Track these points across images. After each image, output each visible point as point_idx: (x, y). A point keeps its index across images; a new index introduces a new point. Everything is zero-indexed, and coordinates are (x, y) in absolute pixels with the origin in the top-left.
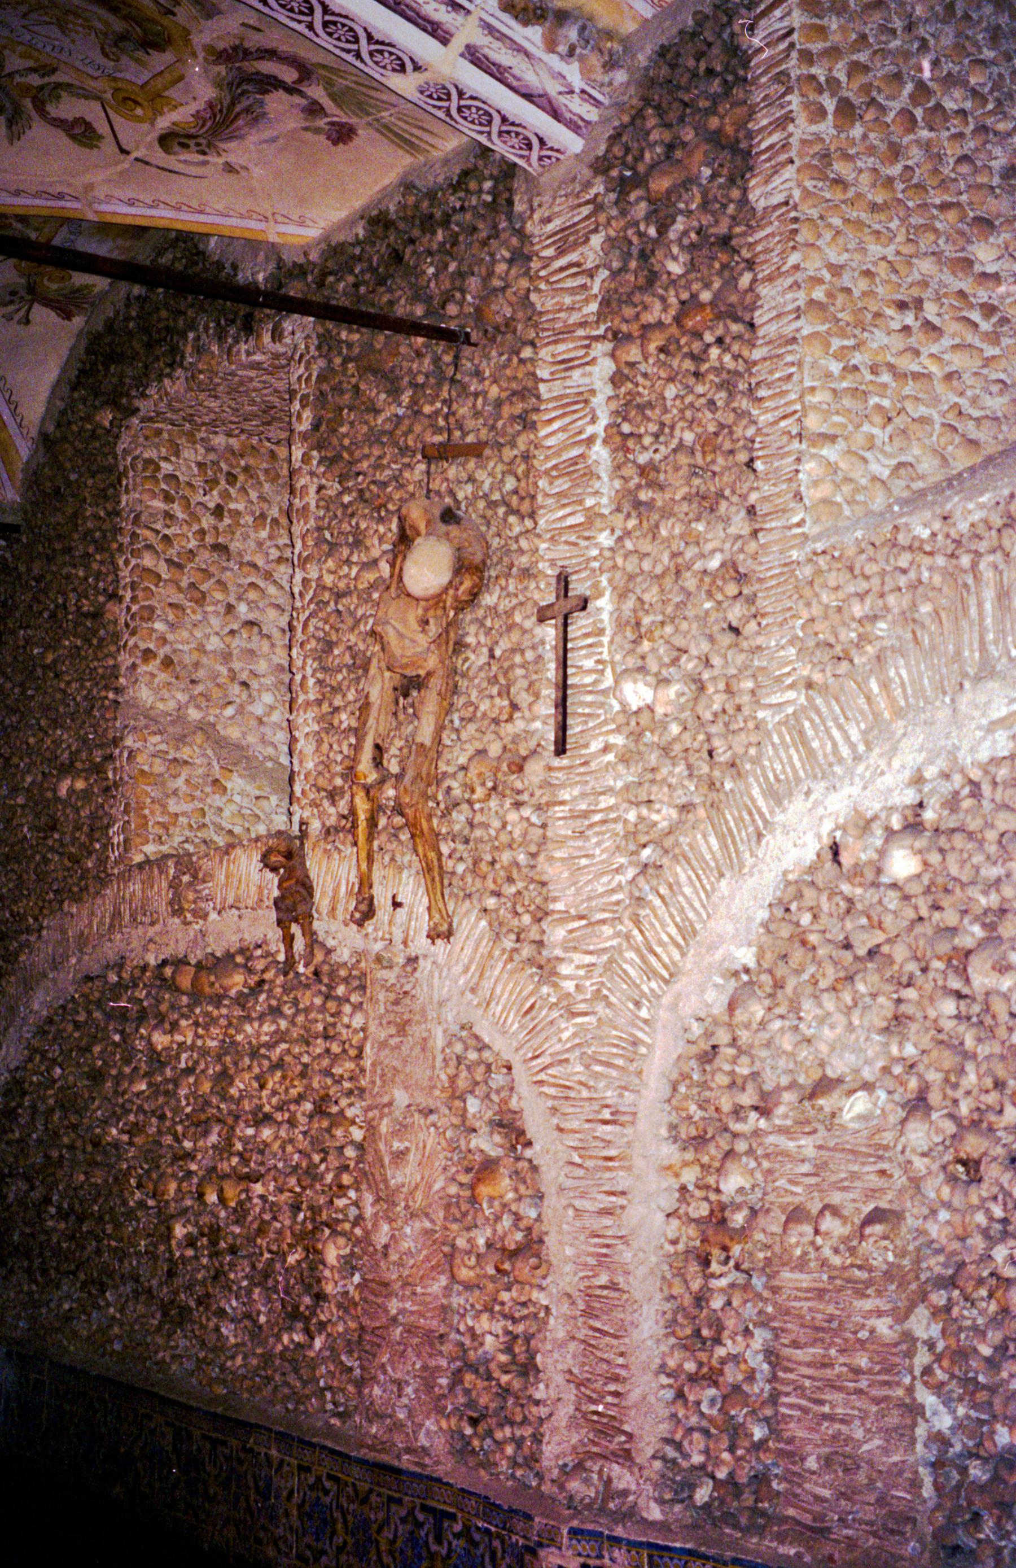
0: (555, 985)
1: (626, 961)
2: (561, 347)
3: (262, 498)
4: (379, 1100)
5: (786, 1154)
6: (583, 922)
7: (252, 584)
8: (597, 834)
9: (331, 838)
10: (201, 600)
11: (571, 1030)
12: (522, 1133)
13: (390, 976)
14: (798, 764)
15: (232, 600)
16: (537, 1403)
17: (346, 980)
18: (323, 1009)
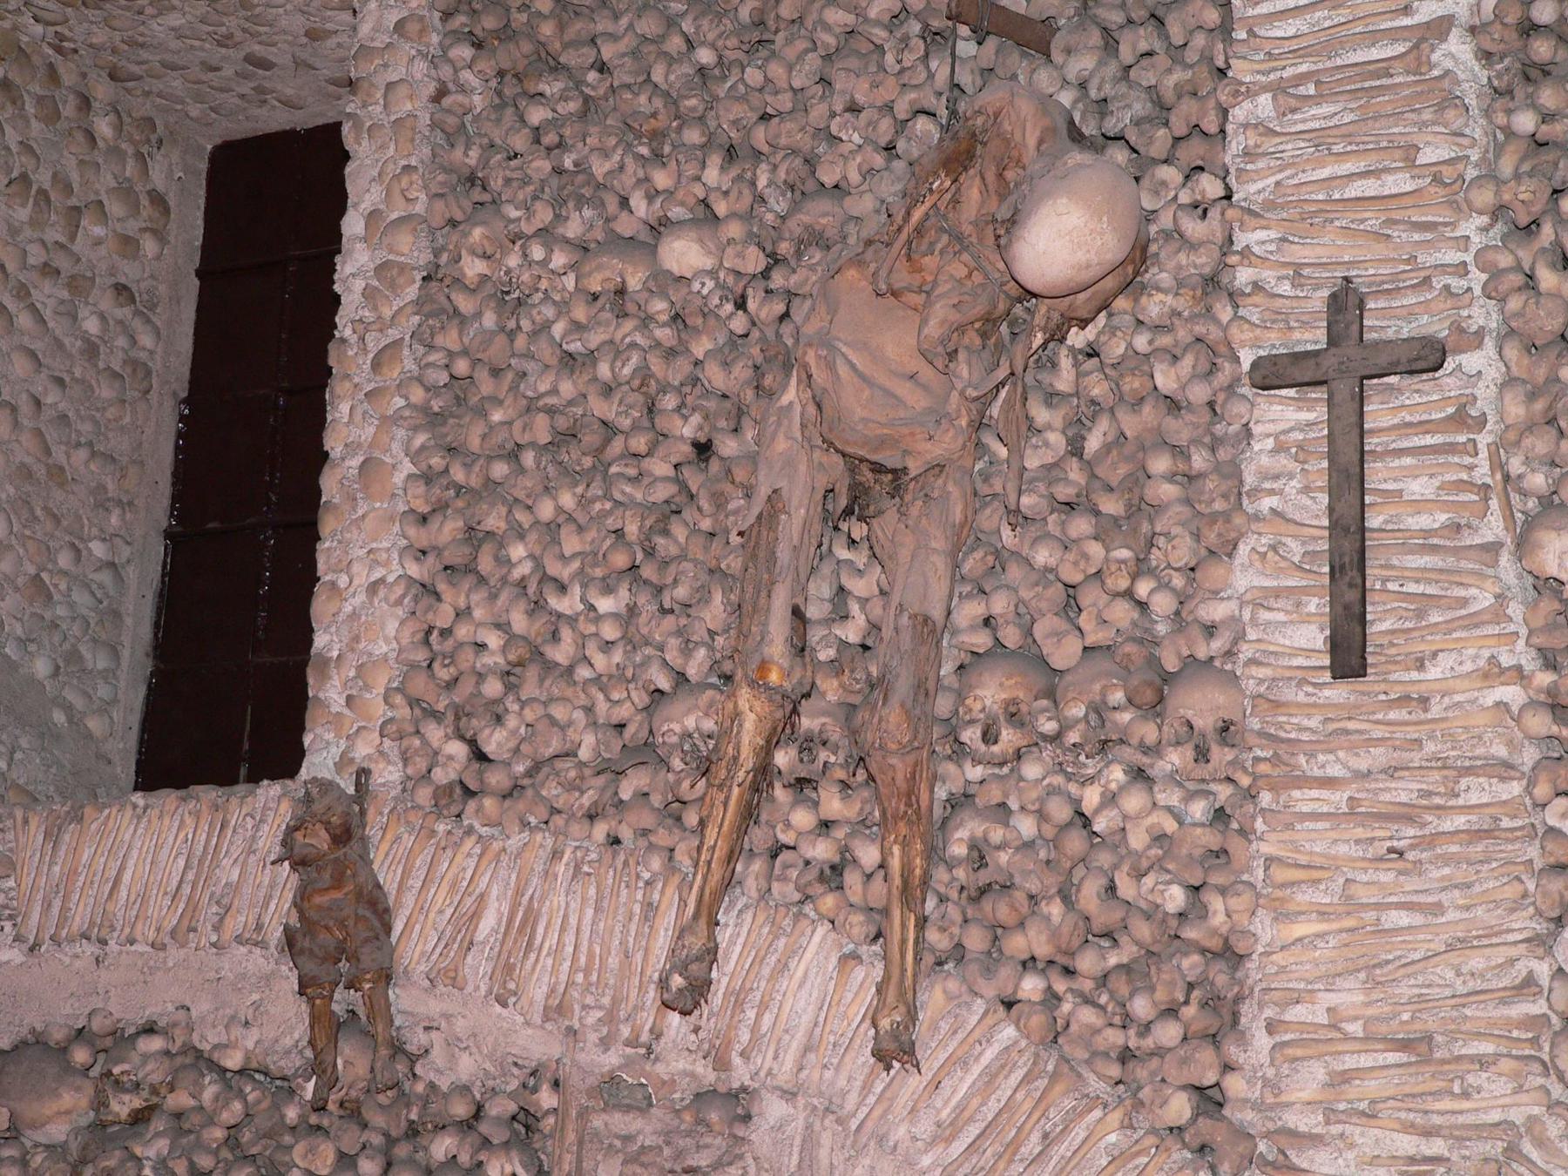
3: (26, 147)
6: (1393, 1057)
8: (1447, 860)
13: (644, 1129)
17: (468, 1125)
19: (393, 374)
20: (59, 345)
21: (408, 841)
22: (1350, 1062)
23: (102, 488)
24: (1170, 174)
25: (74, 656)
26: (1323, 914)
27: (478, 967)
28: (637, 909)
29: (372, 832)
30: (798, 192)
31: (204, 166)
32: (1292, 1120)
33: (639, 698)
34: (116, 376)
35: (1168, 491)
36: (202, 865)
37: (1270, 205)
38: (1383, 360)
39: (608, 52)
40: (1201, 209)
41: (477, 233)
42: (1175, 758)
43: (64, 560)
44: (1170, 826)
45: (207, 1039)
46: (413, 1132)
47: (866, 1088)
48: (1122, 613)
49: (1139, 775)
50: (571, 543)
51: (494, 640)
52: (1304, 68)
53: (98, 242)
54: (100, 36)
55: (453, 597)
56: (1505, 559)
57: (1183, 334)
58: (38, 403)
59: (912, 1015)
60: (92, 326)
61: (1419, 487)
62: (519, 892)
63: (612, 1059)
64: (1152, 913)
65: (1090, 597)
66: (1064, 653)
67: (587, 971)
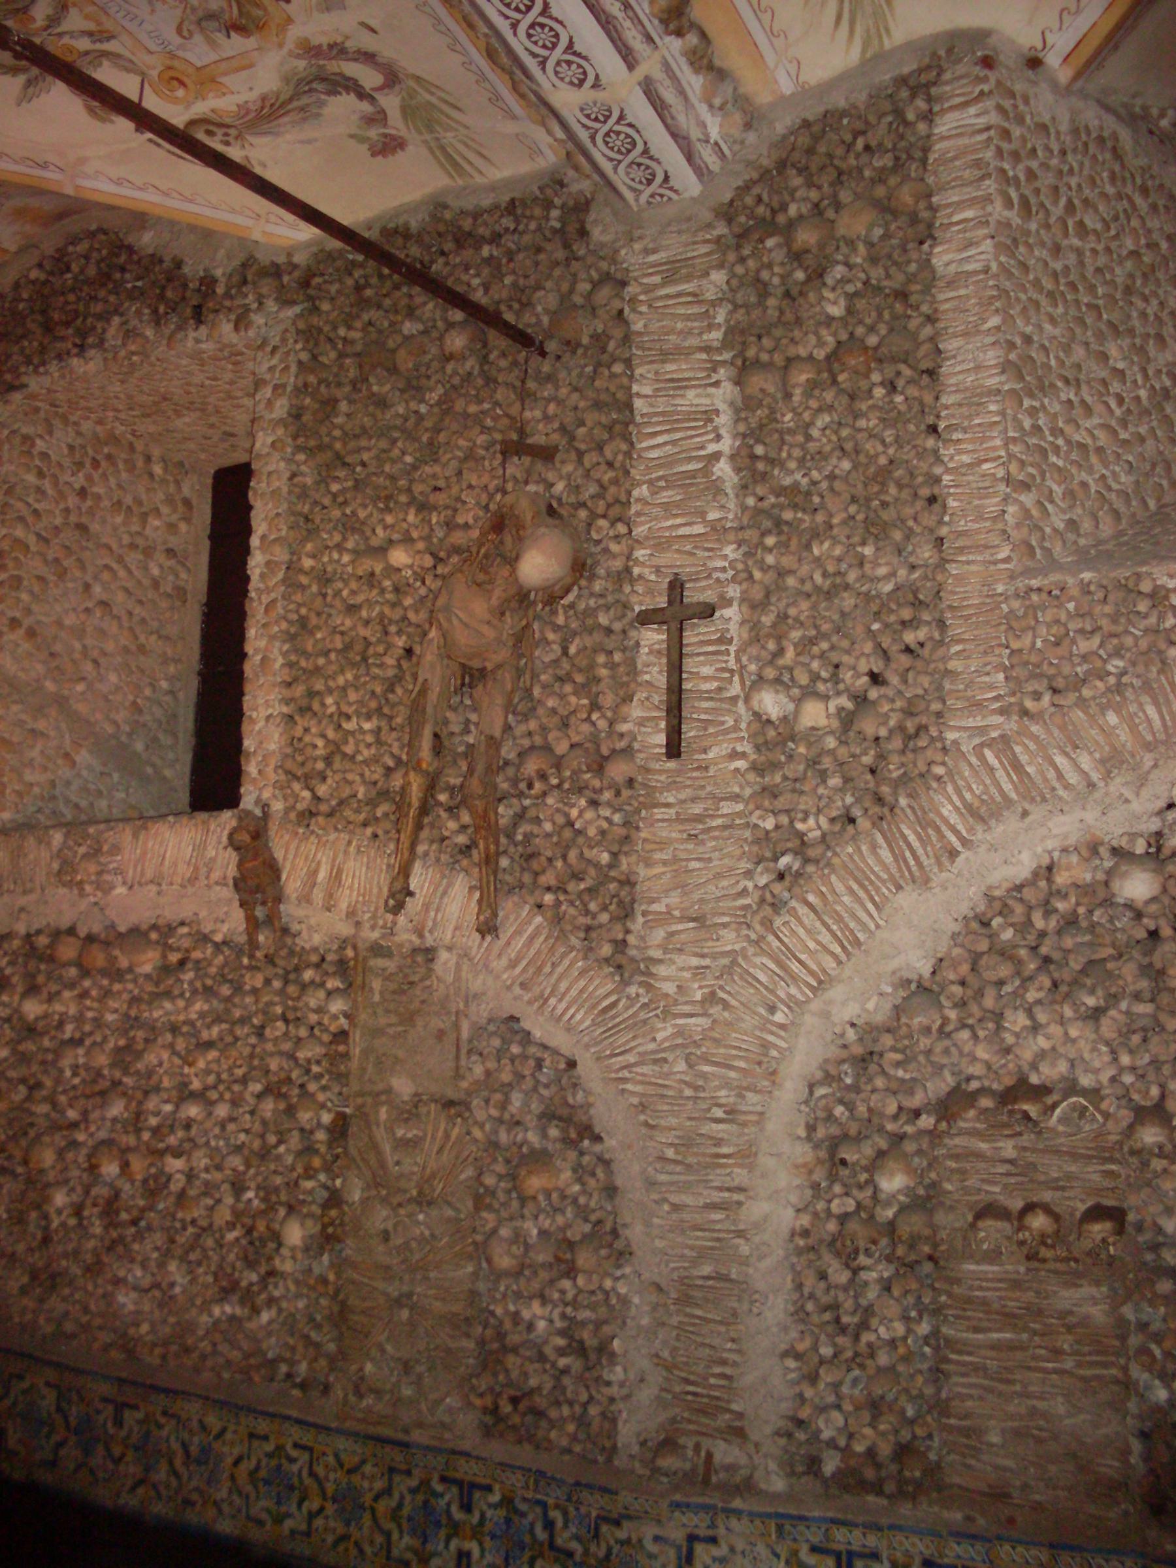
0: (649, 987)
1: (755, 966)
2: (670, 367)
3: (120, 486)
5: (979, 1155)
7: (106, 566)
8: (715, 838)
10: (62, 574)
11: (670, 1031)
13: (390, 965)
14: (1007, 787)
15: (88, 579)
16: (608, 1384)
17: (318, 966)
18: (282, 992)
19: (273, 615)
20: (139, 582)
22: (674, 928)
24: (602, 522)
25: (155, 739)
26: (665, 863)
27: (318, 896)
29: (272, 833)
30: (450, 525)
31: (210, 481)
33: (380, 770)
35: (604, 672)
36: (200, 848)
37: (647, 538)
38: (690, 612)
39: (365, 456)
40: (617, 537)
41: (309, 546)
42: (607, 795)
43: (148, 692)
44: (605, 825)
45: (207, 928)
46: (297, 969)
48: (586, 728)
49: (594, 803)
50: (353, 696)
51: (320, 743)
56: (741, 704)
57: (610, 599)
58: (130, 614)
59: (495, 915)
60: (156, 571)
61: (706, 671)
63: (375, 935)
64: (597, 866)
65: (573, 720)
66: (562, 748)
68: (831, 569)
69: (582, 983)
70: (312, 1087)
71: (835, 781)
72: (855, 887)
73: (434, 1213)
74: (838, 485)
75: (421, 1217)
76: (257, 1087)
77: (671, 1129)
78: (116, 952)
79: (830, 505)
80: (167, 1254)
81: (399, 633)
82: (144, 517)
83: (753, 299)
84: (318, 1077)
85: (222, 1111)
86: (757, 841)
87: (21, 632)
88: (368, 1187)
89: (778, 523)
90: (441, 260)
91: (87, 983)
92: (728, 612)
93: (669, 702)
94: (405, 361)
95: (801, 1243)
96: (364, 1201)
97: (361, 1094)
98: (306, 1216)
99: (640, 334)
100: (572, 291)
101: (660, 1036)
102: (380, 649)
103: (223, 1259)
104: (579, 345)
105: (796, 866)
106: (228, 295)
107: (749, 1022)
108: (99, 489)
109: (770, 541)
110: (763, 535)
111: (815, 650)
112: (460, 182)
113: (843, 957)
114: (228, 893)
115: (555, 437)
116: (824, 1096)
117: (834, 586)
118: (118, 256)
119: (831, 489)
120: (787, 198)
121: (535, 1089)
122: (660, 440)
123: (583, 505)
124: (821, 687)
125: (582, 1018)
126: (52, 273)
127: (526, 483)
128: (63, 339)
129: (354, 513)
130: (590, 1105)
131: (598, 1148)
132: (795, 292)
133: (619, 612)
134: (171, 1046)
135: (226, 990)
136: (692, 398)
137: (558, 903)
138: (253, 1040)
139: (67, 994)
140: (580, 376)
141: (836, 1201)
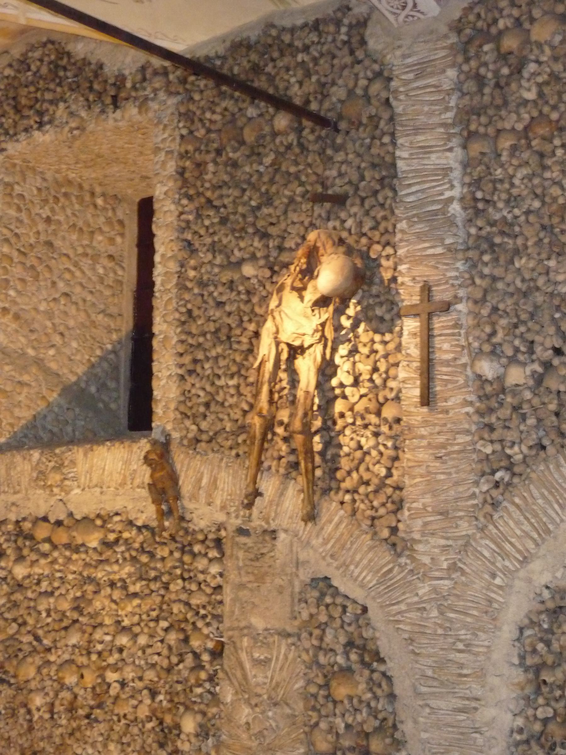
0: (413, 559)
1: (481, 546)
2: (420, 138)
3: (74, 214)
4: (236, 624)
6: (439, 517)
7: (68, 270)
8: (454, 459)
9: (193, 447)
10: (36, 278)
11: (427, 589)
12: (377, 653)
15: (55, 279)
17: (203, 542)
18: (181, 560)
20: (90, 279)
21: (182, 456)
23: (109, 326)
25: (104, 385)
26: (422, 476)
27: (202, 494)
28: (243, 477)
31: (135, 208)
32: (417, 536)
34: (111, 287)
36: (127, 463)
39: (226, 201)
40: (388, 257)
45: (132, 517)
46: (190, 545)
47: (304, 530)
50: (222, 363)
51: (202, 393)
52: (415, 212)
53: (100, 242)
54: (93, 175)
55: (191, 380)
56: (468, 369)
57: (382, 298)
58: (84, 301)
60: (101, 271)
62: (212, 472)
63: (239, 522)
67: (231, 495)
68: (527, 277)
69: (370, 555)
70: (200, 624)
71: (532, 421)
72: (546, 493)
73: (278, 710)
74: (532, 218)
75: (270, 714)
76: (164, 624)
77: (429, 656)
78: (75, 534)
79: (526, 233)
80: (108, 738)
81: (250, 321)
82: (92, 233)
83: (474, 89)
84: (204, 617)
85: (142, 640)
86: (481, 461)
87: (10, 316)
88: (237, 693)
89: (492, 245)
90: (271, 65)
91: (56, 554)
92: (460, 307)
93: (421, 368)
94: (249, 136)
95: (518, 737)
96: (232, 702)
97: (233, 629)
98: (196, 712)
99: (401, 115)
100: (356, 85)
101: (421, 592)
102: (238, 332)
103: (144, 742)
104: (360, 124)
105: (507, 479)
106: (134, 88)
107: (478, 585)
108: (61, 218)
109: (486, 258)
110: (482, 253)
111: (518, 332)
112: (282, 8)
113: (539, 541)
114: (144, 493)
115: (347, 188)
116: (529, 636)
117: (529, 288)
118: (61, 59)
119: (527, 221)
120: (497, 15)
121: (342, 627)
122: (414, 189)
123: (365, 235)
124: (521, 357)
125: (371, 579)
126: (19, 71)
127: (328, 219)
128: (28, 117)
129: (220, 241)
130: (377, 639)
131: (382, 668)
132: (503, 82)
133: (389, 307)
134: (110, 596)
135: (144, 559)
136: (434, 159)
137: (354, 501)
138: (162, 592)
139: (43, 561)
140: (362, 145)
141: (540, 709)
